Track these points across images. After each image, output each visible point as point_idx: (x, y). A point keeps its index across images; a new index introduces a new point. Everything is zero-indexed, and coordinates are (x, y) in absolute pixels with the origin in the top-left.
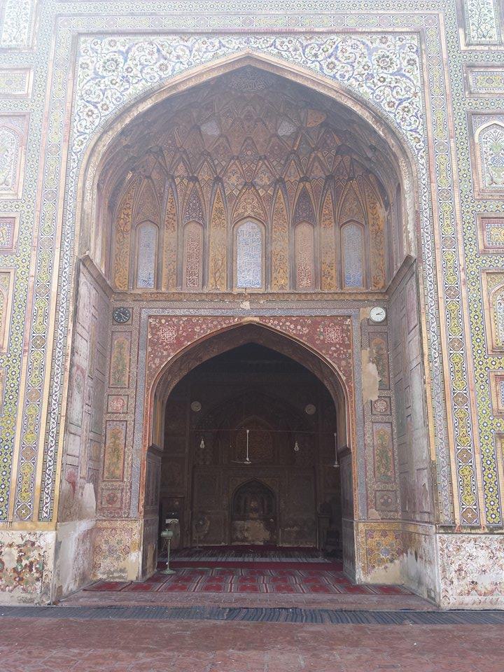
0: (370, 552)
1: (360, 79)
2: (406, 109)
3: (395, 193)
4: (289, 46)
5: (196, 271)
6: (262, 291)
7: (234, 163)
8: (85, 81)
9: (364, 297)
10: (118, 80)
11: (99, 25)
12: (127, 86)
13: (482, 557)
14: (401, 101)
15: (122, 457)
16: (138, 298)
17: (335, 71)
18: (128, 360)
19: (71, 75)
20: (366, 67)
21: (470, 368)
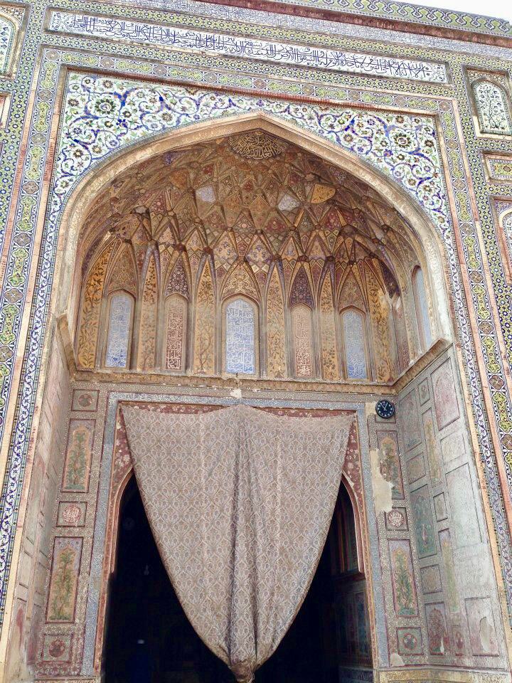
1: (379, 154)
2: (428, 189)
3: (410, 275)
4: (304, 113)
5: (178, 351)
6: (255, 379)
7: (227, 236)
8: (74, 119)
9: (368, 390)
10: (114, 123)
11: (93, 62)
12: (125, 131)
15: (74, 589)
16: (105, 379)
17: (352, 143)
18: (89, 457)
19: (56, 110)
20: (384, 144)
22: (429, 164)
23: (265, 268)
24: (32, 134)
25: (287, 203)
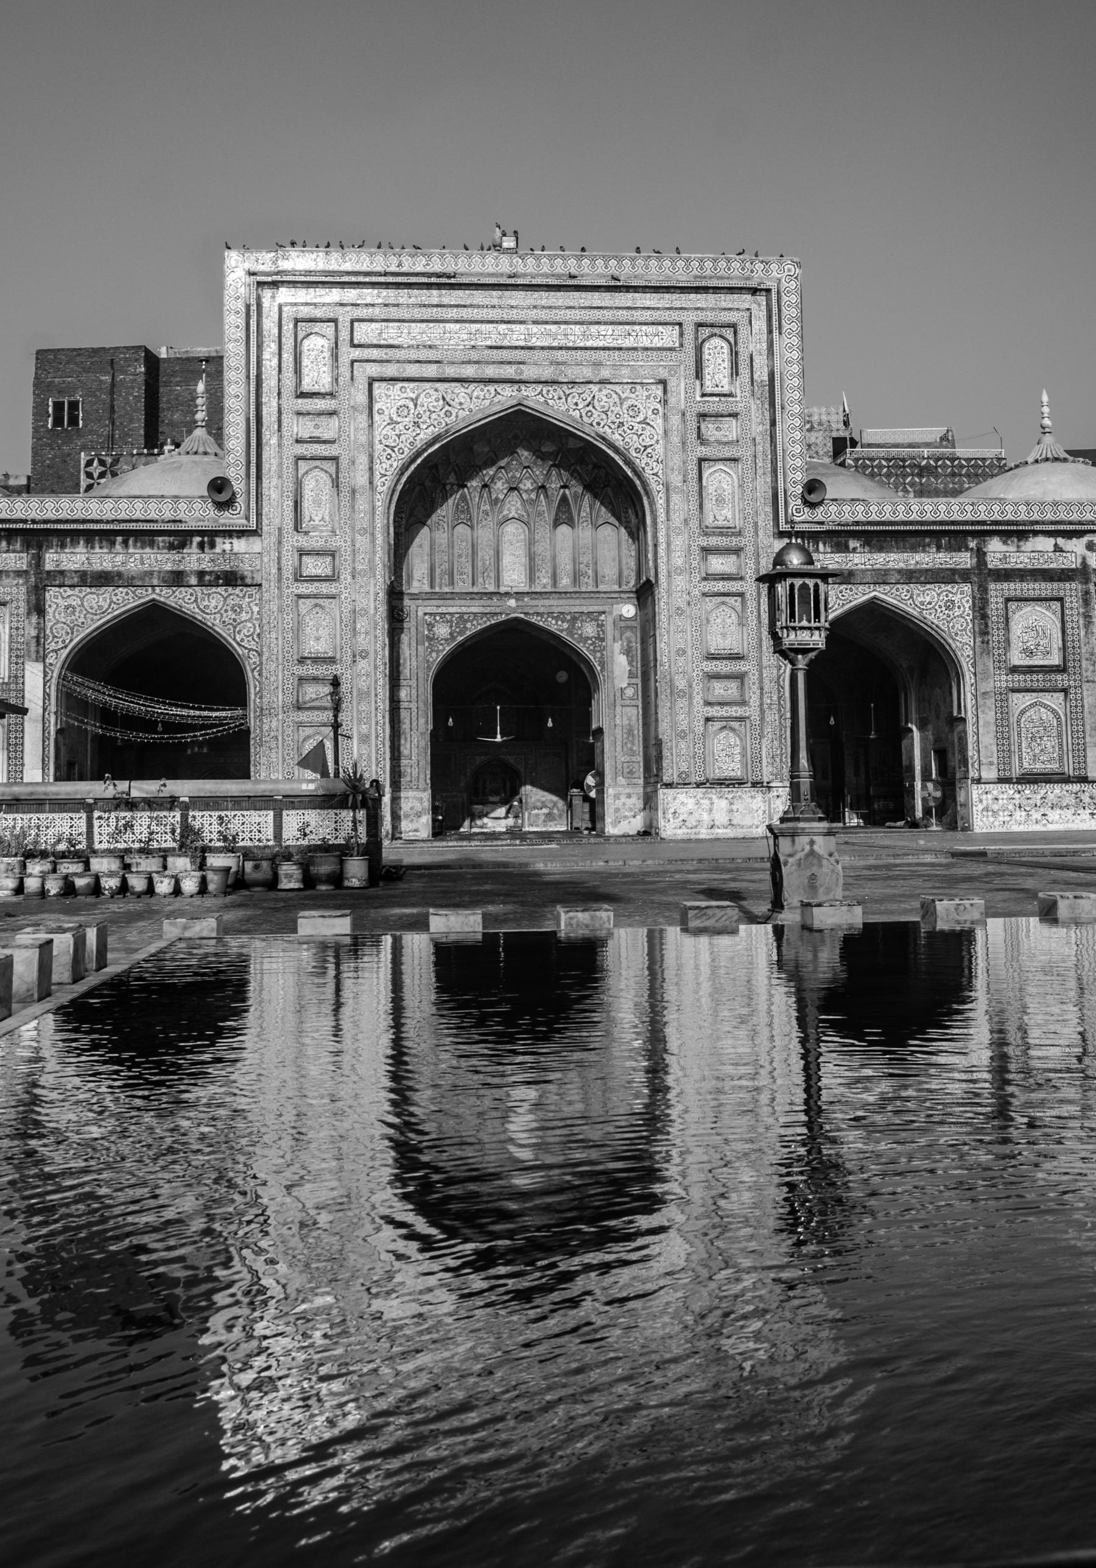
0: (617, 810)
6: (527, 589)
9: (616, 595)
11: (391, 370)
13: (691, 803)
14: (646, 447)
22: (653, 432)
23: (533, 496)
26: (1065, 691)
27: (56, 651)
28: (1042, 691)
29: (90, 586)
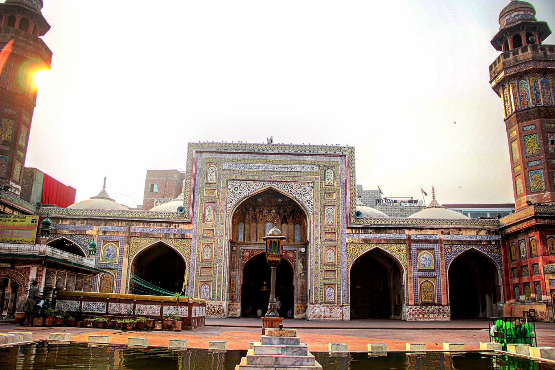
0: (297, 311)
11: (233, 177)
14: (308, 201)
16: (239, 244)
21: (319, 269)
22: (310, 196)
23: (275, 215)
24: (222, 199)
25: (280, 200)
26: (435, 277)
27: (132, 255)
28: (428, 277)
29: (143, 237)
